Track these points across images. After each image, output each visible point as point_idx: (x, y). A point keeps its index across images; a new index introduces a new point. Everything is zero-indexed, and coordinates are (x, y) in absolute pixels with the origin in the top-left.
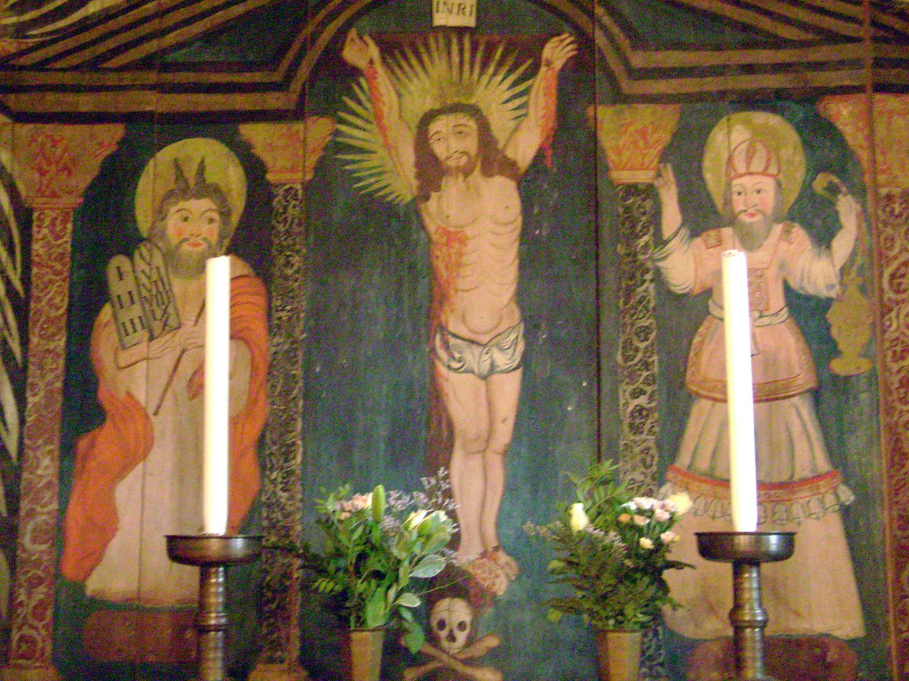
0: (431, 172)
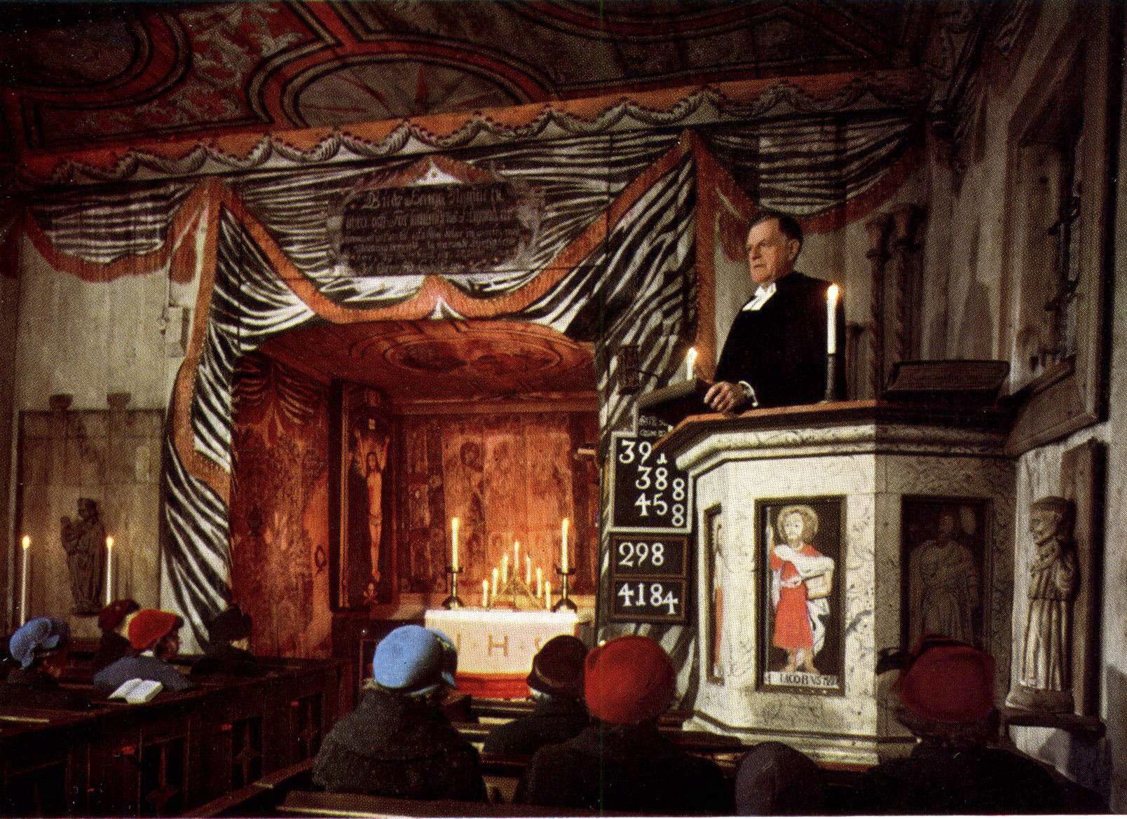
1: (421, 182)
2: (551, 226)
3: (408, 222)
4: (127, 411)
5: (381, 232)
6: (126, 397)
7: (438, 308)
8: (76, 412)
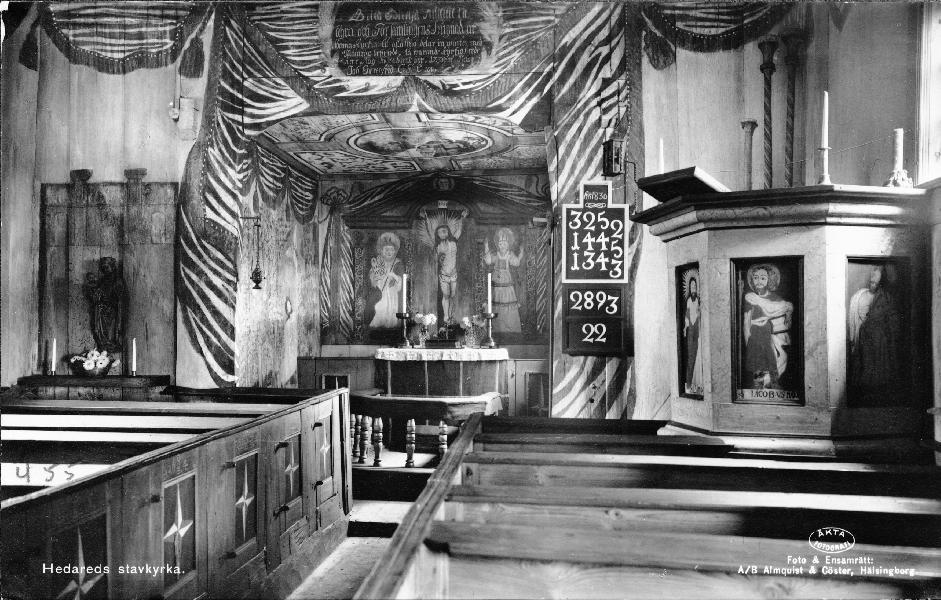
0: (438, 240)
2: (508, 39)
3: (389, 32)
4: (143, 184)
5: (365, 40)
6: (143, 173)
7: (415, 103)
8: (96, 185)
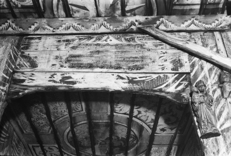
1: (105, 42)
